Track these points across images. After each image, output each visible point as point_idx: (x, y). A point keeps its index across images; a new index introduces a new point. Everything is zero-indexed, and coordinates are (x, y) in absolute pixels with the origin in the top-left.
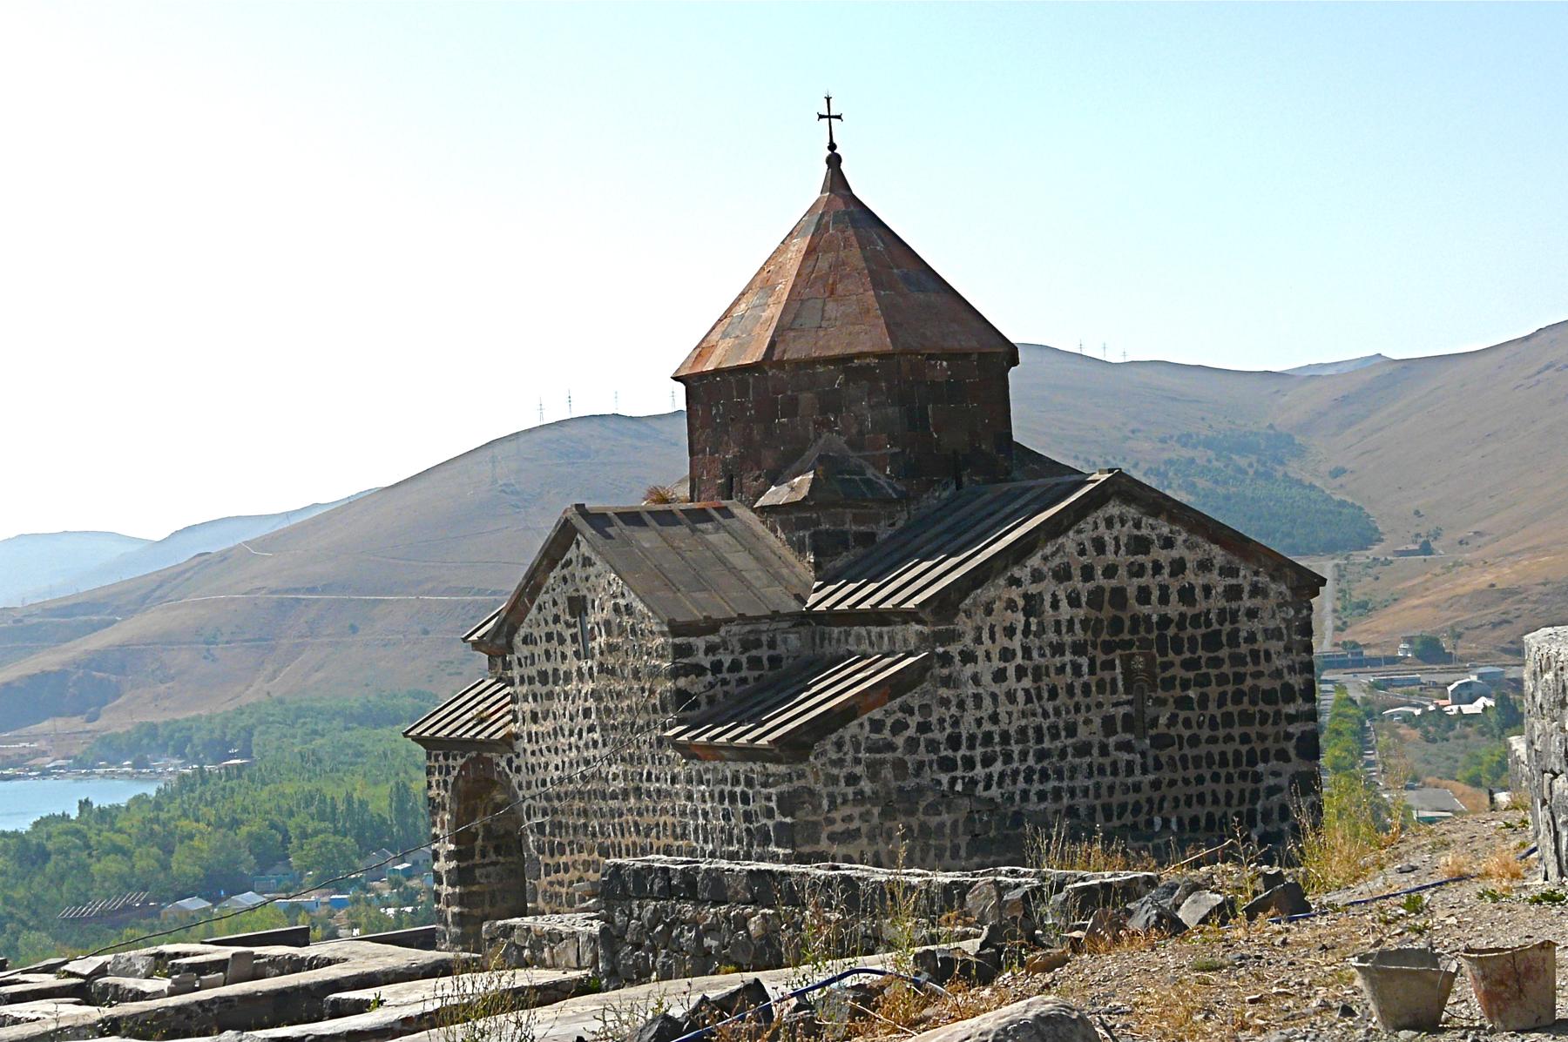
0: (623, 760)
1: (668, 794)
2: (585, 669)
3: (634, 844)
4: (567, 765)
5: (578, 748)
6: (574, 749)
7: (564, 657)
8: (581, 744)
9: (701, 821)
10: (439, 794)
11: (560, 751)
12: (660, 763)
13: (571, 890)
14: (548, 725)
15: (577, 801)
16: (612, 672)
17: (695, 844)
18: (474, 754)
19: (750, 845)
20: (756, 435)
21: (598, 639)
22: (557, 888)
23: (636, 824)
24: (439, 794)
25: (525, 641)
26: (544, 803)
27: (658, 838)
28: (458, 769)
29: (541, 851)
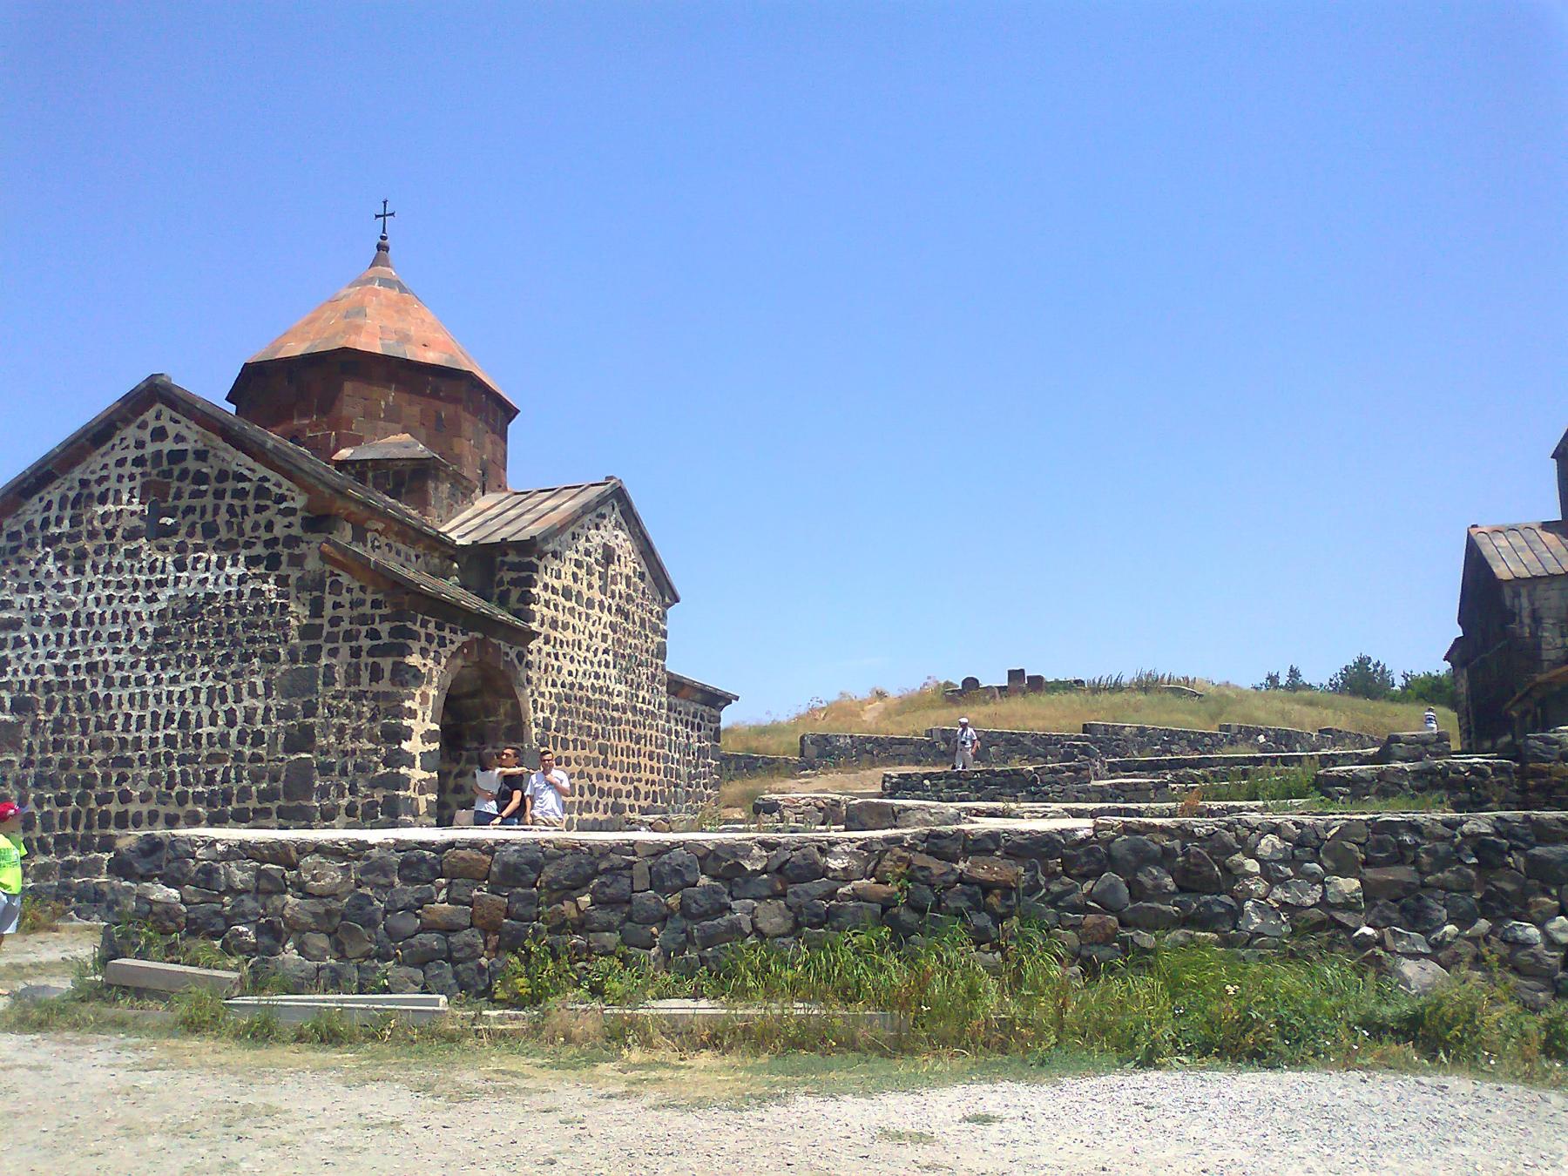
0: (626, 683)
2: (606, 604)
3: (628, 747)
4: (580, 674)
7: (590, 586)
8: (596, 660)
9: (673, 737)
10: (425, 665)
14: (569, 635)
15: (584, 705)
18: (479, 635)
19: (698, 758)
21: (619, 586)
23: (631, 732)
24: (425, 665)
26: (553, 701)
27: (645, 745)
28: (457, 645)
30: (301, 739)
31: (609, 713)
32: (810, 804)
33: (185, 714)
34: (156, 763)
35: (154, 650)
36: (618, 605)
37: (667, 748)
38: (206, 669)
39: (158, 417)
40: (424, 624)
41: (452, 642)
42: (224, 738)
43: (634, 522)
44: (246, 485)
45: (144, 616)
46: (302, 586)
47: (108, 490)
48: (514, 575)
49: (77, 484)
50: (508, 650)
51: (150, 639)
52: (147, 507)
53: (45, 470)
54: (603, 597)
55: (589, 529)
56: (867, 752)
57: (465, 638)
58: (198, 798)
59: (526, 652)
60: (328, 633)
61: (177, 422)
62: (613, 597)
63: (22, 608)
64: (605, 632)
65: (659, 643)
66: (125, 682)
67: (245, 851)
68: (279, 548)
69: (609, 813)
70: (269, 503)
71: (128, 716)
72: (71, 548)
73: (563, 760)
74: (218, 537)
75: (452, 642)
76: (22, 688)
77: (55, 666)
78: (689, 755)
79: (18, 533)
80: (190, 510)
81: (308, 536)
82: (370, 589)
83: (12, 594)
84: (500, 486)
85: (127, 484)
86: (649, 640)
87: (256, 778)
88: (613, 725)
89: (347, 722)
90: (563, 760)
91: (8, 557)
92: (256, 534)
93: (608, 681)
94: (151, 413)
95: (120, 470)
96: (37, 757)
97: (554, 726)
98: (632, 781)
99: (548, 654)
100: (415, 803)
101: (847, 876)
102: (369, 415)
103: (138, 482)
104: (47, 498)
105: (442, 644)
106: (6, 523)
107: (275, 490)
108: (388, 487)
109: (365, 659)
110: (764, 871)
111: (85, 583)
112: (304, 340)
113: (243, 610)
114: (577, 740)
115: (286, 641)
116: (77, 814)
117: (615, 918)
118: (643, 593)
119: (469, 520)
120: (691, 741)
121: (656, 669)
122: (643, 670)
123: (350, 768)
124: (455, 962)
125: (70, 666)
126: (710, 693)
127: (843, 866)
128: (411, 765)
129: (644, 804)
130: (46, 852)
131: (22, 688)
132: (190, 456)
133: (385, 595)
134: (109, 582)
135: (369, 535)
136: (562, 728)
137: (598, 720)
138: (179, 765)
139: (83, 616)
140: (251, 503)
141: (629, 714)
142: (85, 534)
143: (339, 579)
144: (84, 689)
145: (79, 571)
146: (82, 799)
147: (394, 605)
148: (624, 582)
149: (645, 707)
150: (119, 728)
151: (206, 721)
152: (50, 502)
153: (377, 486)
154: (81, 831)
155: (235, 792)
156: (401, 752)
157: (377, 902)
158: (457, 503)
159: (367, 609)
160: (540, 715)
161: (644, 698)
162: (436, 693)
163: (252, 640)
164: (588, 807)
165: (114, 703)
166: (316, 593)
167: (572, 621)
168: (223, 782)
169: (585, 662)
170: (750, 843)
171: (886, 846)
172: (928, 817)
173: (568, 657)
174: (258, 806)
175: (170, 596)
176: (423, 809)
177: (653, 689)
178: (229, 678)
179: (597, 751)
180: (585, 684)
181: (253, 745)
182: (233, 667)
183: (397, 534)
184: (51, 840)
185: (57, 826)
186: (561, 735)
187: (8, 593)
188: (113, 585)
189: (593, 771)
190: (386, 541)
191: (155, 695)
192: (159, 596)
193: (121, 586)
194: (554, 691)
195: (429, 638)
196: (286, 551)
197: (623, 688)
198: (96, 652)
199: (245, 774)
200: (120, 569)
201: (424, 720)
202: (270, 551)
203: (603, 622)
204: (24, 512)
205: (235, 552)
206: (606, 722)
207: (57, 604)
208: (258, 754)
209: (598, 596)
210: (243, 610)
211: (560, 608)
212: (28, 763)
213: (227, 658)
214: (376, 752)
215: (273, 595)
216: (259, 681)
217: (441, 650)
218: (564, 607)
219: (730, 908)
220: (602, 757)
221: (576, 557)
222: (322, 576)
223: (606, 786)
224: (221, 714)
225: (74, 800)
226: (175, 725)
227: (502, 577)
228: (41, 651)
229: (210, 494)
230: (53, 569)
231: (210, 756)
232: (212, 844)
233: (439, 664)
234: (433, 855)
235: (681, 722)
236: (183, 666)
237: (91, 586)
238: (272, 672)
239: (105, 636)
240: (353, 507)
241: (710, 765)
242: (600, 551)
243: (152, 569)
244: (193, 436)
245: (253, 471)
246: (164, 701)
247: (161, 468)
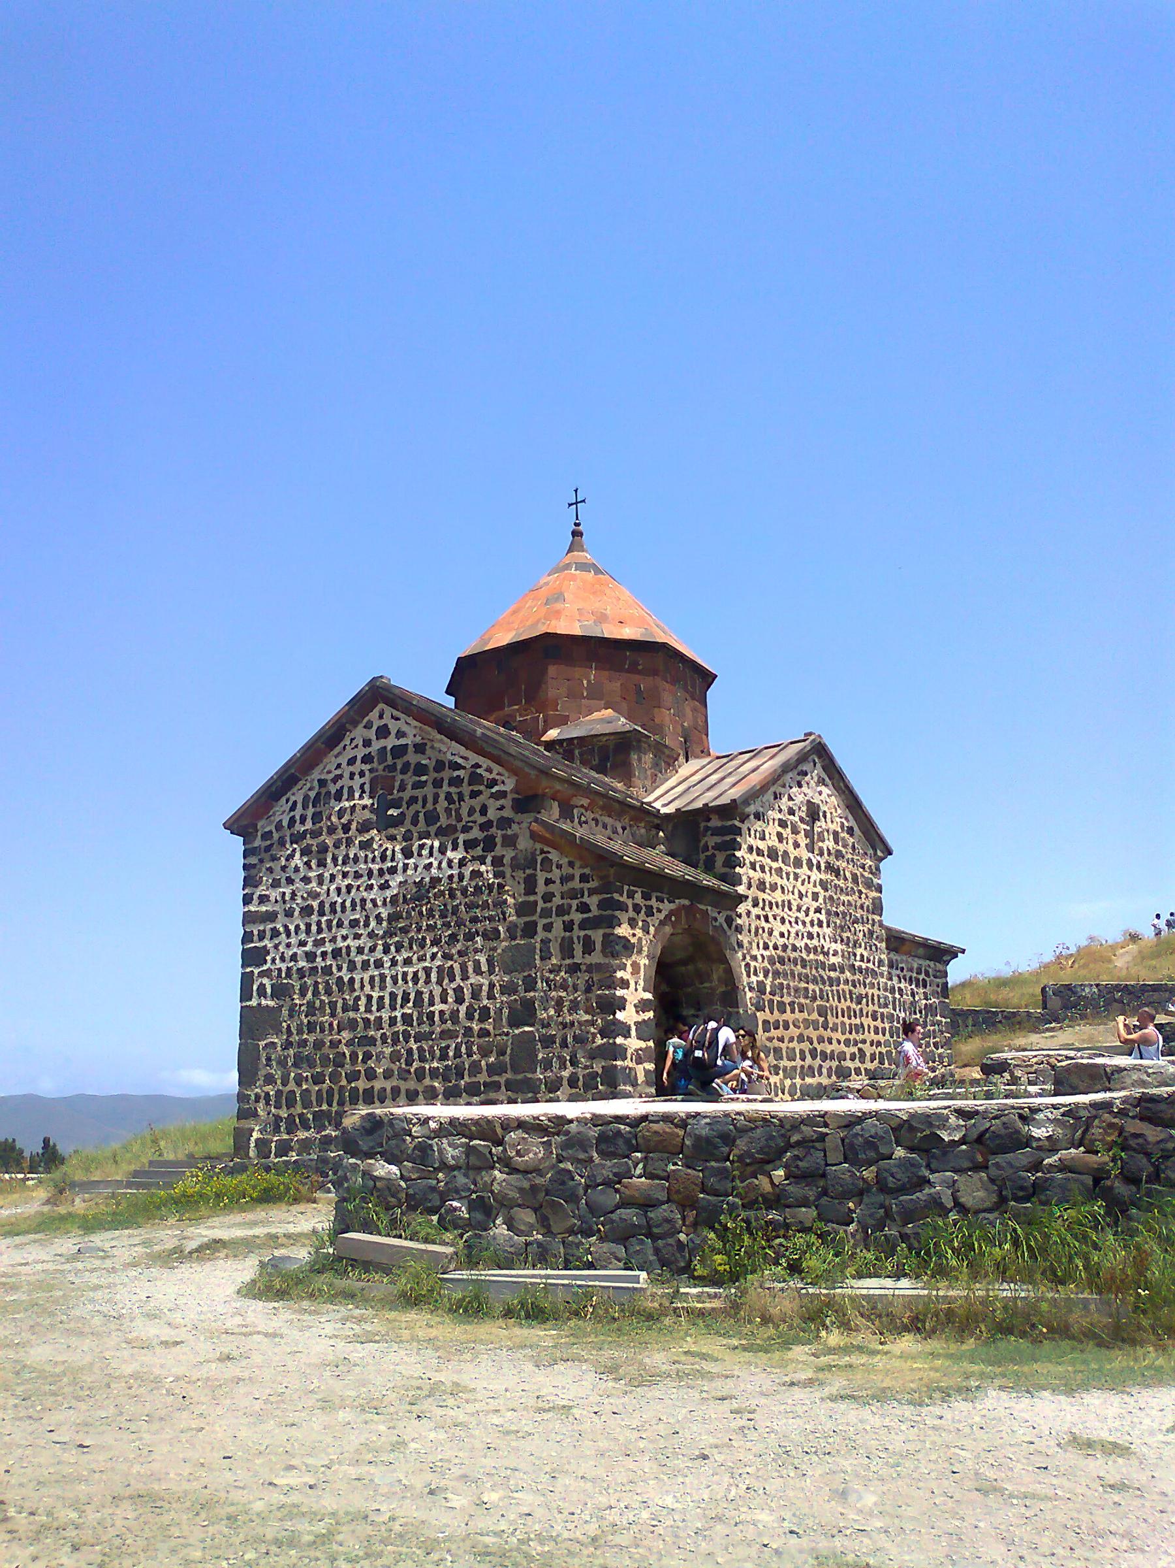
0: (842, 941)
1: (874, 972)
2: (815, 862)
3: (849, 1008)
4: (793, 935)
5: (804, 923)
6: (800, 923)
7: (796, 845)
8: (807, 920)
9: (897, 996)
11: (787, 922)
12: (871, 949)
13: (791, 1045)
14: (778, 896)
15: (799, 967)
17: (892, 1012)
18: (687, 902)
19: (926, 1016)
20: (699, 720)
21: (827, 842)
22: (776, 1043)
23: (850, 992)
24: (634, 935)
26: (766, 964)
27: (868, 1005)
30: (524, 1013)
31: (825, 974)
32: (1042, 1063)
33: (419, 994)
34: (395, 1041)
35: (389, 933)
36: (827, 862)
37: (891, 1006)
38: (435, 950)
39: (381, 717)
40: (631, 895)
41: (659, 911)
42: (454, 1014)
43: (837, 776)
44: (461, 773)
45: (379, 903)
46: (515, 866)
47: (342, 787)
48: (718, 839)
49: (316, 784)
51: (385, 924)
52: (376, 800)
53: (289, 773)
54: (810, 855)
55: (791, 788)
56: (1115, 1000)
57: (672, 906)
58: (434, 1073)
59: (734, 916)
60: (542, 909)
61: (397, 719)
62: (821, 854)
63: (276, 901)
64: (816, 890)
65: (874, 899)
66: (365, 965)
67: (455, 1127)
68: (493, 830)
69: (834, 1078)
70: (482, 788)
71: (369, 998)
72: (314, 842)
73: (781, 1023)
74: (439, 824)
75: (659, 911)
76: (279, 975)
77: (306, 953)
78: (915, 1013)
79: (271, 832)
80: (413, 800)
81: (518, 817)
82: (577, 864)
83: (268, 889)
84: (702, 752)
85: (358, 781)
86: (863, 896)
87: (485, 1053)
88: (831, 986)
89: (564, 994)
91: (263, 855)
92: (471, 819)
93: (822, 940)
94: (376, 713)
95: (351, 768)
96: (295, 1038)
97: (768, 989)
98: (856, 1043)
99: (758, 917)
100: (633, 1073)
101: (1052, 1145)
102: (573, 695)
103: (367, 779)
104: (293, 798)
105: (650, 910)
106: (259, 825)
107: (486, 775)
108: (594, 763)
109: (577, 933)
110: (963, 1141)
111: (327, 875)
112: (510, 630)
113: (464, 892)
114: (794, 1002)
115: (505, 919)
116: (330, 1091)
117: (811, 1194)
118: (853, 848)
119: (673, 788)
120: (917, 998)
121: (873, 925)
122: (859, 927)
123: (570, 1040)
124: (654, 1238)
125: (319, 953)
126: (933, 947)
127: (1047, 1135)
128: (627, 1035)
129: (871, 1066)
130: (308, 1128)
131: (279, 975)
132: (411, 749)
133: (592, 869)
134: (348, 872)
135: (575, 811)
136: (778, 991)
137: (815, 981)
138: (415, 1042)
139: (327, 906)
140: (466, 789)
141: (848, 974)
142: (325, 829)
143: (550, 856)
144: (331, 973)
145: (322, 864)
146: (334, 1077)
147: (601, 878)
148: (831, 837)
149: (864, 966)
150: (362, 1009)
151: (437, 999)
152: (295, 803)
153: (584, 763)
154: (335, 1108)
155: (467, 1066)
156: (616, 1022)
157: (577, 1177)
158: (661, 772)
159: (576, 884)
160: (754, 979)
161: (862, 956)
162: (647, 962)
163: (475, 920)
164: (811, 1071)
165: (357, 986)
166: (528, 871)
167: (779, 882)
168: (455, 1057)
169: (797, 923)
170: (945, 1112)
171: (1094, 1112)
172: (1145, 1077)
173: (778, 918)
174: (488, 1080)
175: (401, 882)
176: (641, 1078)
177: (871, 946)
178: (456, 957)
179: (816, 1014)
180: (798, 945)
181: (481, 1021)
182: (459, 946)
183: (603, 808)
184: (310, 1116)
185: (315, 1103)
186: (777, 998)
187: (265, 888)
188: (351, 875)
189: (812, 1033)
190: (592, 816)
191: (392, 977)
192: (390, 883)
193: (357, 875)
194: (766, 953)
195: (637, 909)
196: (499, 832)
197: (838, 947)
198: (339, 939)
199: (475, 1048)
200: (356, 860)
201: (636, 990)
202: (485, 833)
203: (812, 880)
204: (274, 814)
205: (453, 837)
206: (824, 983)
207: (305, 895)
208: (486, 1029)
209: (805, 855)
210: (464, 892)
211: (767, 869)
212: (288, 1045)
213: (453, 938)
214: (592, 1023)
215: (491, 876)
216: (483, 959)
217: (649, 919)
218: (771, 868)
219: (929, 1181)
220: (822, 1019)
221: (779, 816)
222: (533, 854)
223: (829, 1049)
224: (450, 992)
225: (327, 1078)
226: (410, 1004)
227: (707, 842)
228: (293, 940)
229: (430, 784)
230: (300, 864)
231: (442, 1032)
232: (425, 1121)
233: (648, 933)
234: (628, 1129)
235: (905, 980)
236: (415, 948)
237: (333, 878)
238: (494, 949)
239: (346, 923)
240: (558, 786)
241: (939, 1023)
242: (804, 808)
243: (383, 858)
244: (412, 731)
245: (466, 759)
246: (400, 981)
247: (385, 764)
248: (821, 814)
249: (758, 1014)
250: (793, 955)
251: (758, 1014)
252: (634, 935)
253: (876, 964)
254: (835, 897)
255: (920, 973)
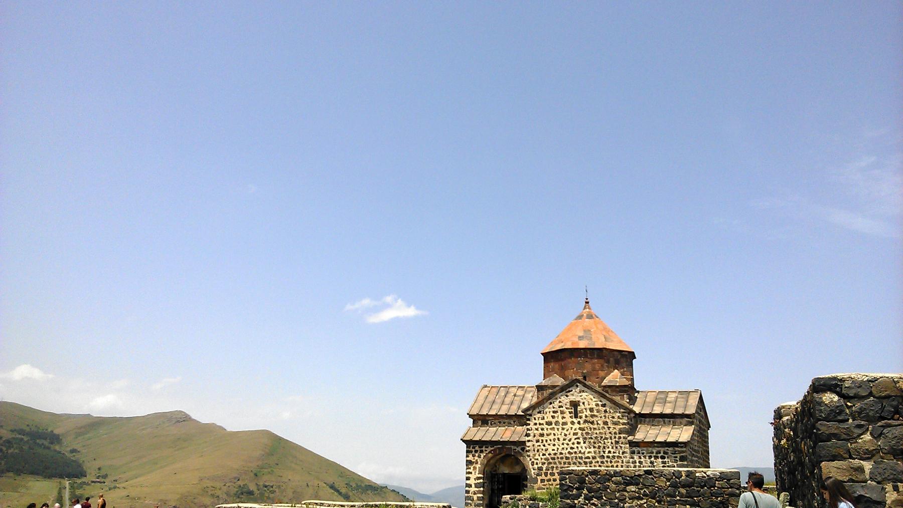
0: (594, 447)
6: (565, 446)
9: (638, 464)
12: (617, 448)
14: (552, 437)
16: (592, 423)
21: (585, 413)
25: (539, 412)
29: (538, 475)
40: (473, 448)
41: (486, 451)
50: (516, 448)
54: (574, 420)
57: (492, 448)
62: (581, 417)
64: (576, 432)
65: (620, 429)
73: (552, 479)
90: (552, 479)
97: (544, 469)
99: (540, 446)
118: (605, 411)
135: (489, 422)
148: (588, 411)
160: (536, 466)
162: (480, 466)
194: (543, 457)
197: (592, 450)
203: (573, 429)
211: (545, 429)
218: (547, 429)
221: (553, 410)
235: (645, 457)
248: (581, 404)
249: (538, 477)
250: (560, 456)
251: (538, 477)
252: (474, 459)
253: (621, 453)
254: (590, 432)
255: (660, 453)
